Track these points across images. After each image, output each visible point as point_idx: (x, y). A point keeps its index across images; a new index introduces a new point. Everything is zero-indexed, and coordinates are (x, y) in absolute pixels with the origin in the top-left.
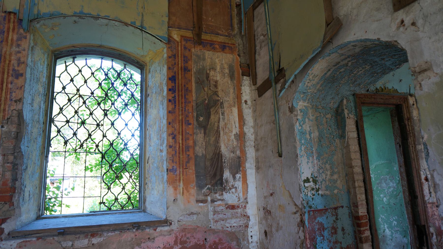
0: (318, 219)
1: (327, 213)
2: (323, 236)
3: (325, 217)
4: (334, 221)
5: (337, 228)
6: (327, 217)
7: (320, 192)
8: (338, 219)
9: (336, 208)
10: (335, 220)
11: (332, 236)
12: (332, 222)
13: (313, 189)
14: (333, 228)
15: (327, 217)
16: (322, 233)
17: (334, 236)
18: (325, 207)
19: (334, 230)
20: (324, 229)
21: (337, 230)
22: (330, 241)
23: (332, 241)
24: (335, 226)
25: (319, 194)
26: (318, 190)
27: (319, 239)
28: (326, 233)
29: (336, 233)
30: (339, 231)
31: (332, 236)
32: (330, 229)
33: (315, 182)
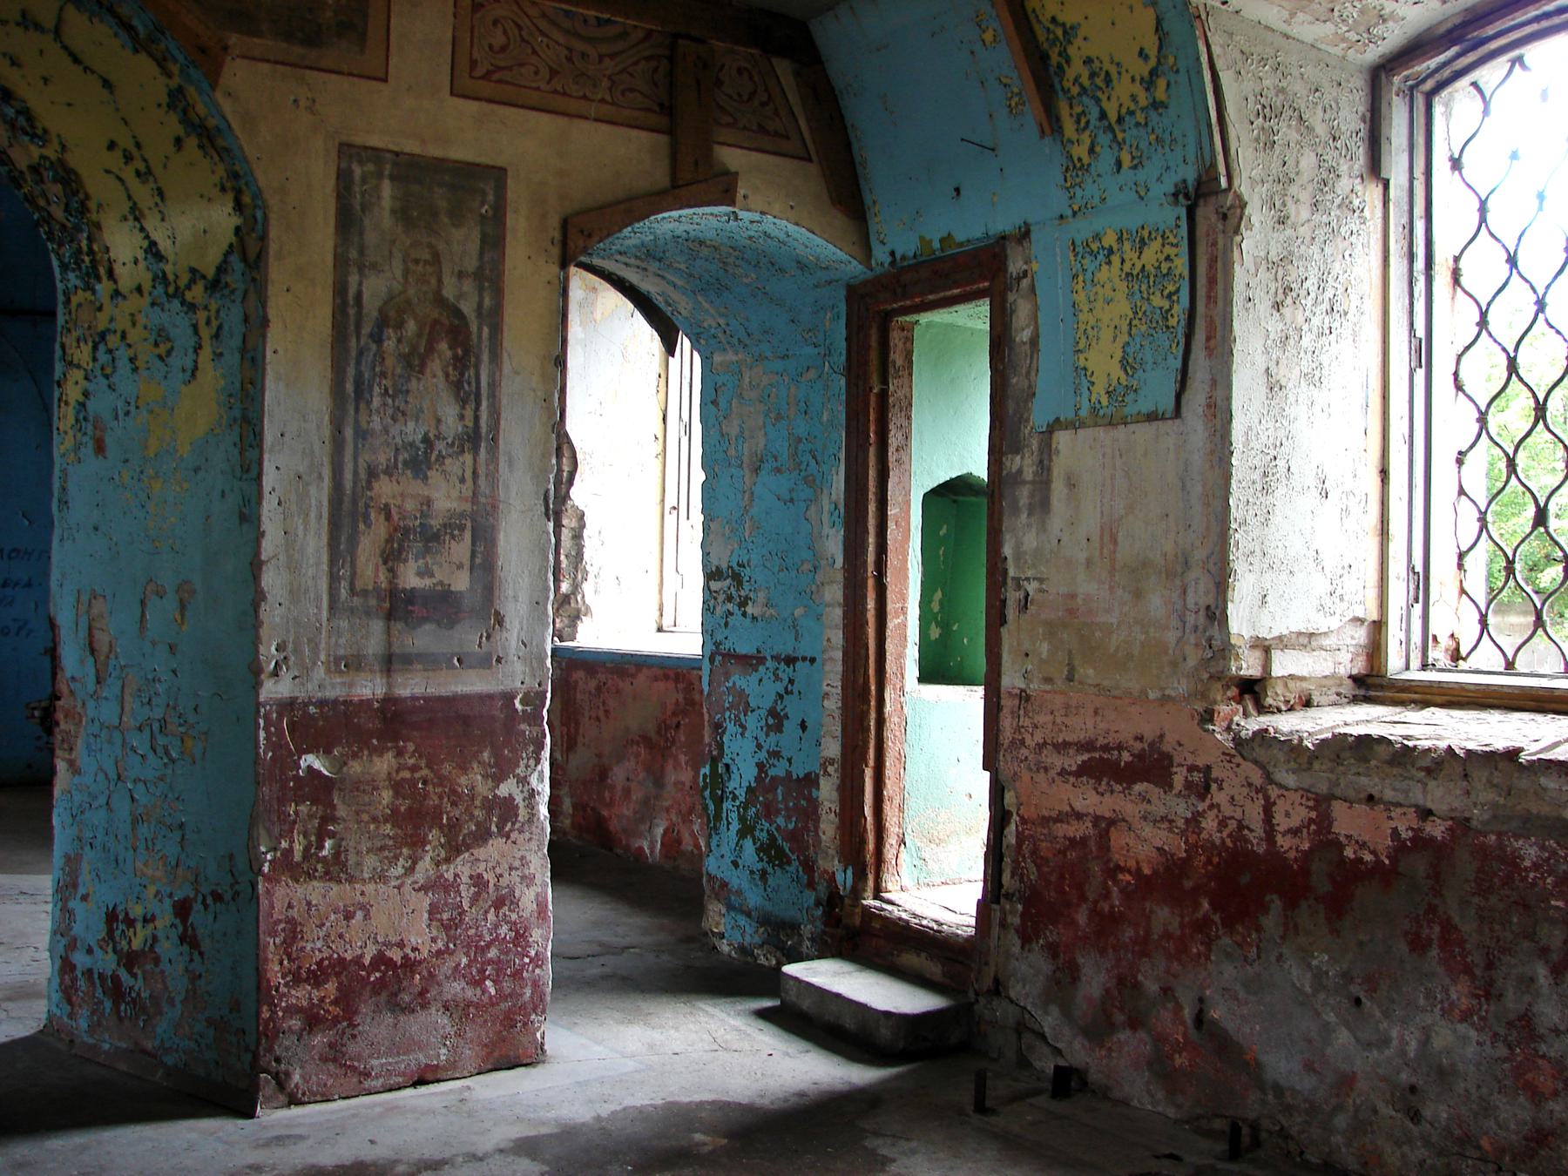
0: (735, 678)
1: (762, 669)
2: (743, 727)
3: (755, 677)
4: (781, 697)
5: (786, 717)
6: (761, 680)
7: (749, 609)
8: (792, 693)
9: (790, 661)
10: (783, 692)
11: (767, 735)
12: (773, 697)
13: (730, 599)
14: (772, 713)
15: (761, 680)
16: (742, 716)
17: (772, 734)
18: (759, 652)
19: (776, 720)
20: (748, 709)
21: (785, 722)
22: (759, 747)
23: (766, 747)
24: (779, 709)
25: (744, 614)
26: (743, 603)
27: (731, 728)
28: (752, 722)
29: (778, 728)
30: (790, 726)
31: (767, 735)
32: (763, 713)
33: (737, 579)
